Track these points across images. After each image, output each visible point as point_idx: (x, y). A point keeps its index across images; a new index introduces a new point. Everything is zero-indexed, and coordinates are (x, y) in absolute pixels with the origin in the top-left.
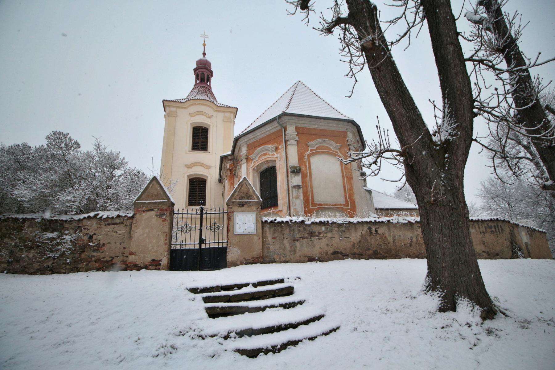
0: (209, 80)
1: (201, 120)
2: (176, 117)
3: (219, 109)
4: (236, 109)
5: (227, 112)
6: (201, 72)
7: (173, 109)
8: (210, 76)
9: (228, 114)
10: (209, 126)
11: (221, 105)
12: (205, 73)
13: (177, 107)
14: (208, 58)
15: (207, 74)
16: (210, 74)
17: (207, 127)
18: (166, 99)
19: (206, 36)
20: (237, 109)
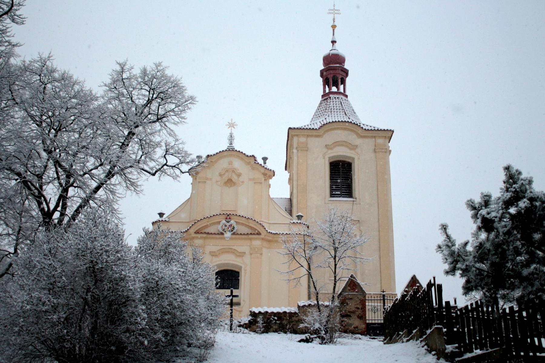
0: (343, 82)
1: (341, 153)
2: (307, 150)
3: (367, 134)
4: (391, 133)
5: (380, 137)
6: (332, 75)
7: (303, 139)
8: (344, 78)
9: (380, 141)
10: (353, 159)
11: (370, 128)
12: (338, 75)
13: (308, 136)
14: (340, 49)
15: (340, 77)
16: (344, 74)
17: (350, 161)
18: (292, 127)
19: (336, 12)
20: (393, 131)
